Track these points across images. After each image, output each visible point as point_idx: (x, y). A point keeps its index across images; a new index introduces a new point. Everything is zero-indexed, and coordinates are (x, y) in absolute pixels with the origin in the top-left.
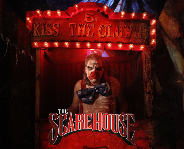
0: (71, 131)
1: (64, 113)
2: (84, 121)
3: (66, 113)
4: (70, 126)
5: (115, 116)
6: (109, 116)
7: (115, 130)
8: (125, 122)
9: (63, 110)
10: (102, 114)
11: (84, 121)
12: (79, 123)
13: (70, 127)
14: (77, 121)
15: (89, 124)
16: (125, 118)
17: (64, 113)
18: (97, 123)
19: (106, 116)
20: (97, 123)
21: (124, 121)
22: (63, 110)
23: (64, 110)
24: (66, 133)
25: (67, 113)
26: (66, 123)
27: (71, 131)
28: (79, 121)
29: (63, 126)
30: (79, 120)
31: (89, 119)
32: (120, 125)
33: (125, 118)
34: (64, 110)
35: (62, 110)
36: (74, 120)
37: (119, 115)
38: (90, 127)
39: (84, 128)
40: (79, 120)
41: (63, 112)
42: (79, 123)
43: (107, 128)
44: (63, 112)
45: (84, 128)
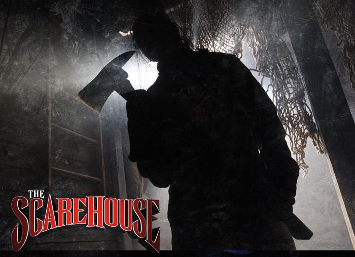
0: (50, 227)
1: (38, 196)
2: (72, 211)
3: (41, 197)
6: (115, 201)
7: (127, 226)
8: (144, 212)
9: (36, 192)
10: (104, 199)
11: (72, 211)
12: (65, 214)
13: (47, 220)
14: (61, 211)
15: (81, 216)
16: (144, 205)
17: (38, 196)
18: (96, 215)
19: (111, 202)
20: (96, 215)
21: (141, 211)
22: (36, 192)
23: (38, 191)
24: (42, 231)
25: (43, 197)
26: (41, 214)
27: (50, 227)
28: (64, 211)
29: (36, 219)
30: (65, 208)
31: (81, 206)
32: (135, 218)
33: (144, 205)
34: (38, 191)
35: (35, 191)
36: (55, 209)
37: (133, 201)
39: (72, 222)
41: (36, 194)
43: (111, 222)
44: (36, 194)
45: (72, 222)
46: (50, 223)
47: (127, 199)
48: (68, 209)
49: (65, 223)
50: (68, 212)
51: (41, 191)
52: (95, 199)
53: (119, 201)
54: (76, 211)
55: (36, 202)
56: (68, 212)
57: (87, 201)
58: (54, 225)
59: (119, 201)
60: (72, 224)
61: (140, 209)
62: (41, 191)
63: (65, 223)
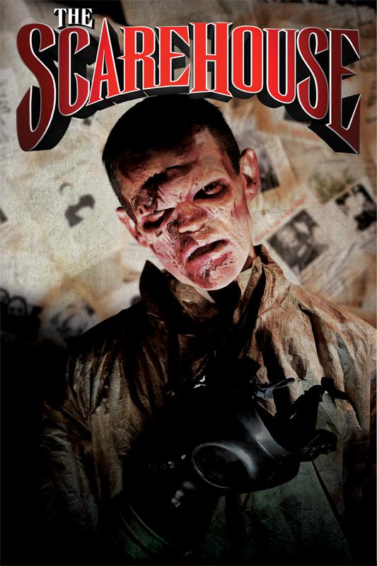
1: (77, 22)
2: (156, 56)
3: (84, 22)
4: (102, 74)
6: (256, 33)
7: (283, 91)
8: (323, 58)
9: (74, 12)
10: (231, 28)
11: (156, 56)
12: (140, 64)
13: (98, 77)
14: (131, 57)
15: (179, 64)
16: (323, 43)
17: (77, 22)
19: (248, 35)
21: (316, 56)
22: (74, 12)
23: (77, 10)
24: (87, 102)
25: (90, 25)
26: (81, 62)
27: (104, 94)
28: (138, 57)
29: (73, 77)
30: (139, 49)
31: (177, 42)
32: (302, 72)
33: (323, 43)
34: (77, 10)
35: (70, 10)
36: (118, 52)
39: (157, 83)
40: (139, 49)
41: (73, 18)
42: (140, 64)
44: (73, 18)
45: (157, 83)
46: (104, 84)
49: (140, 85)
51: (84, 11)
53: (265, 33)
54: (168, 55)
55: (74, 36)
56: (146, 59)
58: (114, 90)
59: (265, 33)
60: (157, 87)
61: (313, 51)
62: (84, 11)
63: (140, 85)
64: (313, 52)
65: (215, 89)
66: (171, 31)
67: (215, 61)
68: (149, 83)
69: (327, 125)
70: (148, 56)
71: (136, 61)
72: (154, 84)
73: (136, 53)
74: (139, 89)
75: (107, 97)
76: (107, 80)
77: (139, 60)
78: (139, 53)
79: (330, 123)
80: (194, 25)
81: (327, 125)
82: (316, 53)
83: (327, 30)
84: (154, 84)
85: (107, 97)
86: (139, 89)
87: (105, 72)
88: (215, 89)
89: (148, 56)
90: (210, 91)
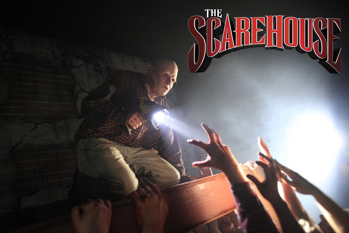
0: (227, 48)
1: (215, 15)
2: (250, 30)
3: (218, 16)
4: (226, 39)
5: (307, 21)
6: (295, 20)
7: (307, 46)
8: (324, 31)
9: (214, 11)
10: (284, 18)
11: (250, 30)
12: (243, 34)
13: (225, 40)
14: (239, 31)
15: (260, 35)
16: (325, 25)
17: (215, 15)
18: (275, 35)
19: (291, 21)
20: (275, 35)
21: (322, 31)
22: (214, 11)
23: (215, 10)
24: (220, 51)
25: (221, 17)
26: (218, 33)
27: (227, 48)
28: (242, 31)
29: (213, 40)
30: (243, 28)
31: (260, 25)
32: (315, 38)
33: (325, 25)
34: (215, 10)
35: (212, 10)
36: (233, 29)
37: (314, 20)
38: (263, 41)
39: (251, 43)
40: (243, 28)
41: (214, 14)
42: (243, 34)
43: (291, 42)
44: (214, 14)
45: (251, 43)
46: (227, 43)
47: (307, 19)
48: (247, 29)
49: (243, 43)
50: (247, 33)
51: (218, 10)
52: (275, 18)
53: (299, 20)
54: (255, 30)
55: (214, 22)
56: (246, 32)
57: (266, 20)
58: (232, 46)
59: (299, 20)
60: (251, 44)
61: (320, 28)
62: (218, 10)
63: (243, 43)
64: (320, 29)
65: (277, 45)
66: (257, 19)
67: (277, 33)
68: (247, 43)
69: (326, 61)
70: (247, 30)
71: (241, 33)
72: (250, 43)
73: (241, 29)
74: (243, 45)
75: (228, 49)
76: (229, 41)
77: (243, 32)
78: (243, 29)
79: (328, 60)
80: (267, 17)
81: (326, 61)
82: (321, 29)
83: (326, 19)
84: (250, 43)
85: (228, 49)
86: (243, 45)
87: (227, 38)
88: (277, 45)
89: (247, 30)
90: (274, 46)
